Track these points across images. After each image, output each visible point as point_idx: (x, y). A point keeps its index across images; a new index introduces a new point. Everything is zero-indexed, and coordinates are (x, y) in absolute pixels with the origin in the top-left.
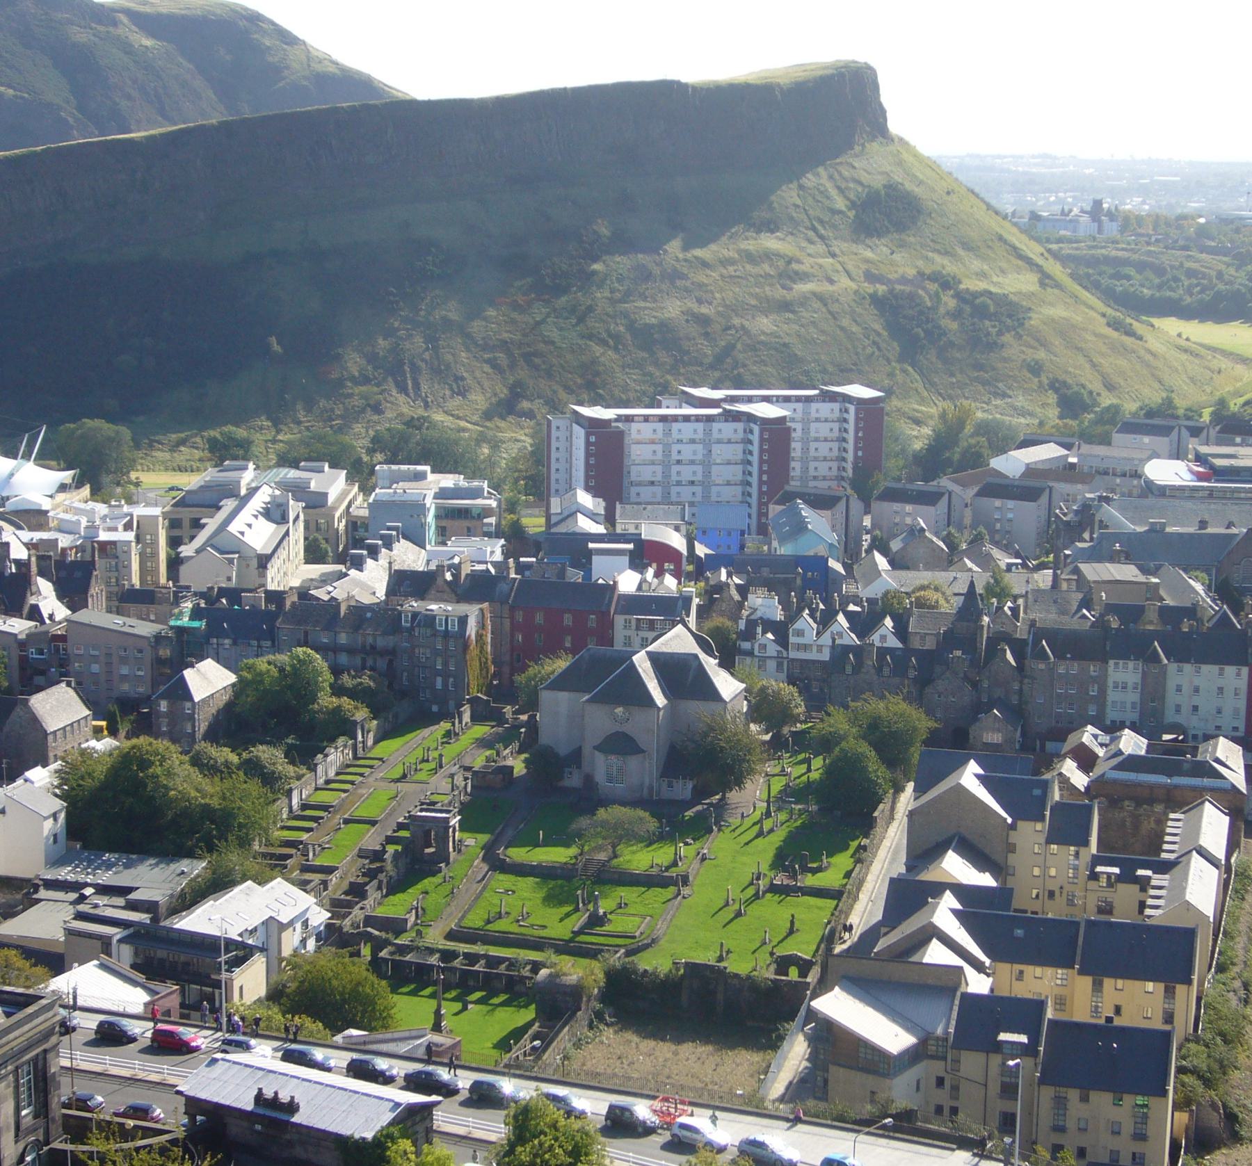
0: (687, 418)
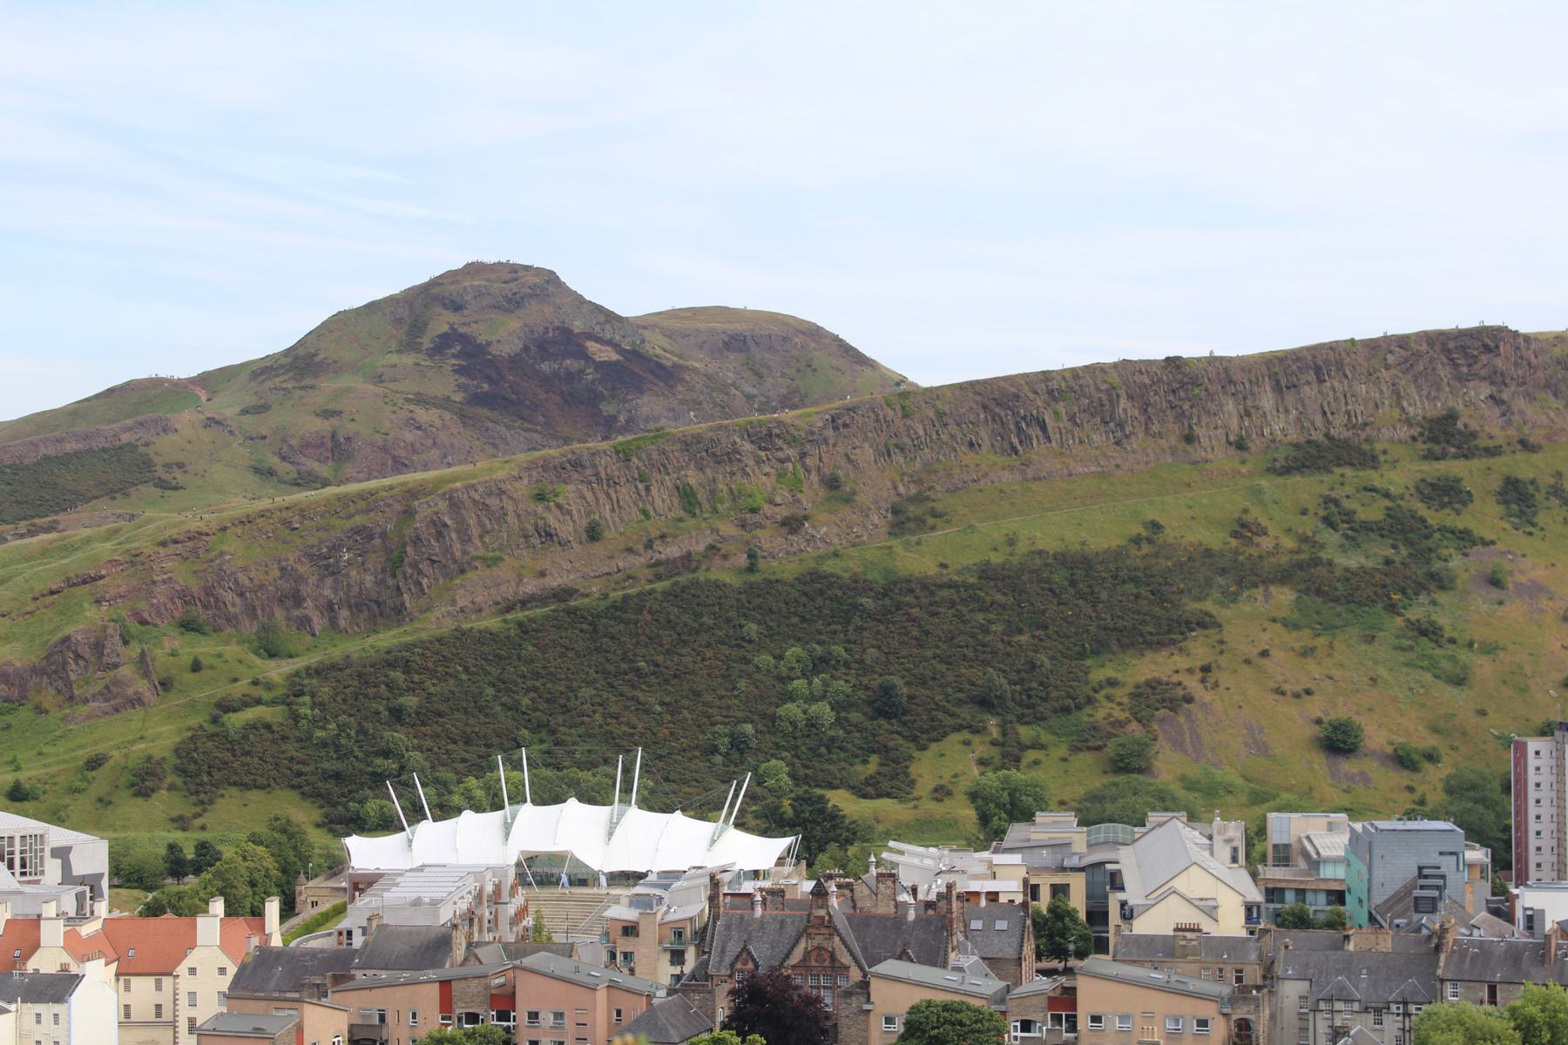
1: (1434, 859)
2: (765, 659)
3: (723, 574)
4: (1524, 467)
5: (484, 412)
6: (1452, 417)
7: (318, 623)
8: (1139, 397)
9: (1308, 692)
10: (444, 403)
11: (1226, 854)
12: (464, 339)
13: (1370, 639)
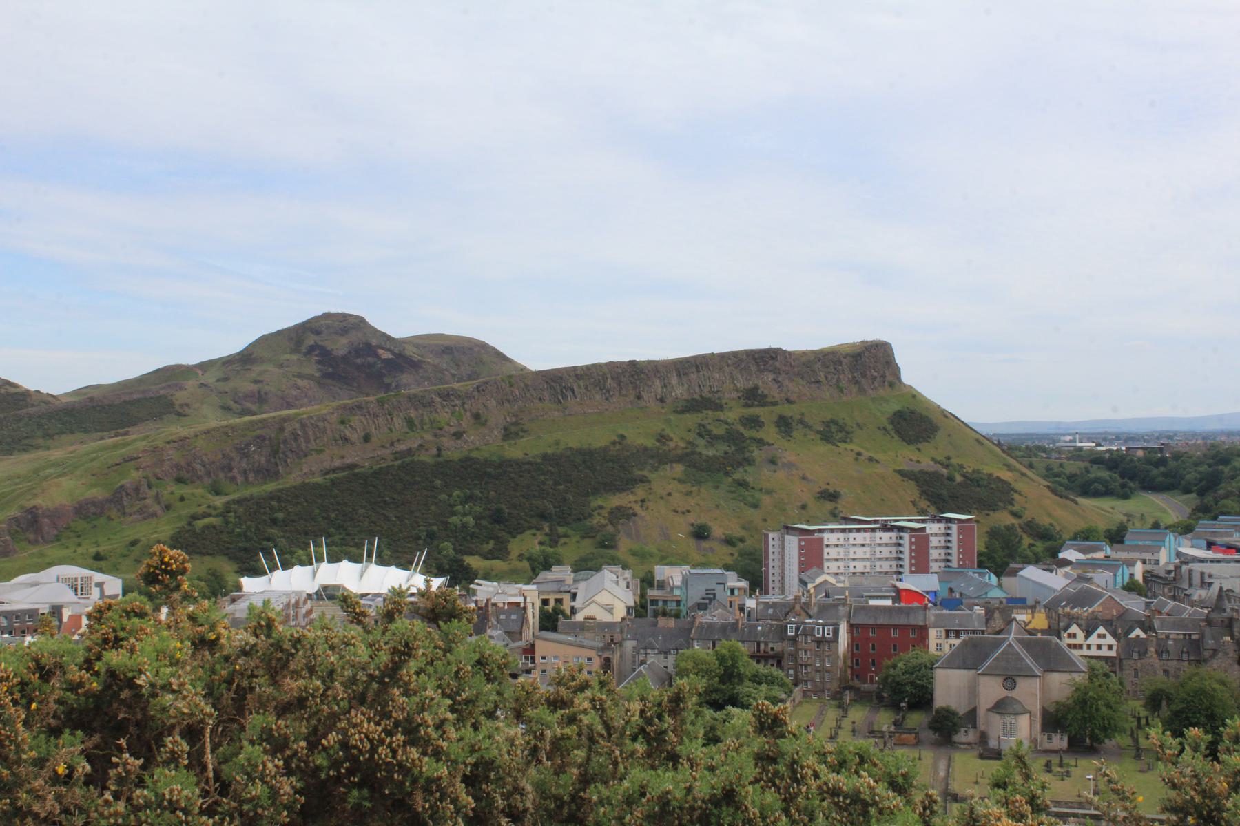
0: (858, 530)
1: (713, 586)
2: (443, 496)
3: (425, 457)
4: (787, 410)
5: (329, 381)
6: (756, 388)
7: (240, 479)
9: (688, 511)
10: (311, 377)
11: (623, 584)
12: (322, 348)
13: (717, 487)
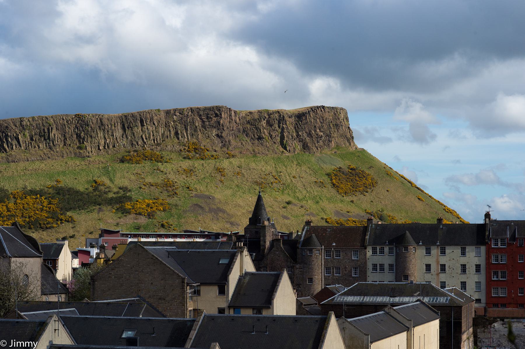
8: (62, 129)
